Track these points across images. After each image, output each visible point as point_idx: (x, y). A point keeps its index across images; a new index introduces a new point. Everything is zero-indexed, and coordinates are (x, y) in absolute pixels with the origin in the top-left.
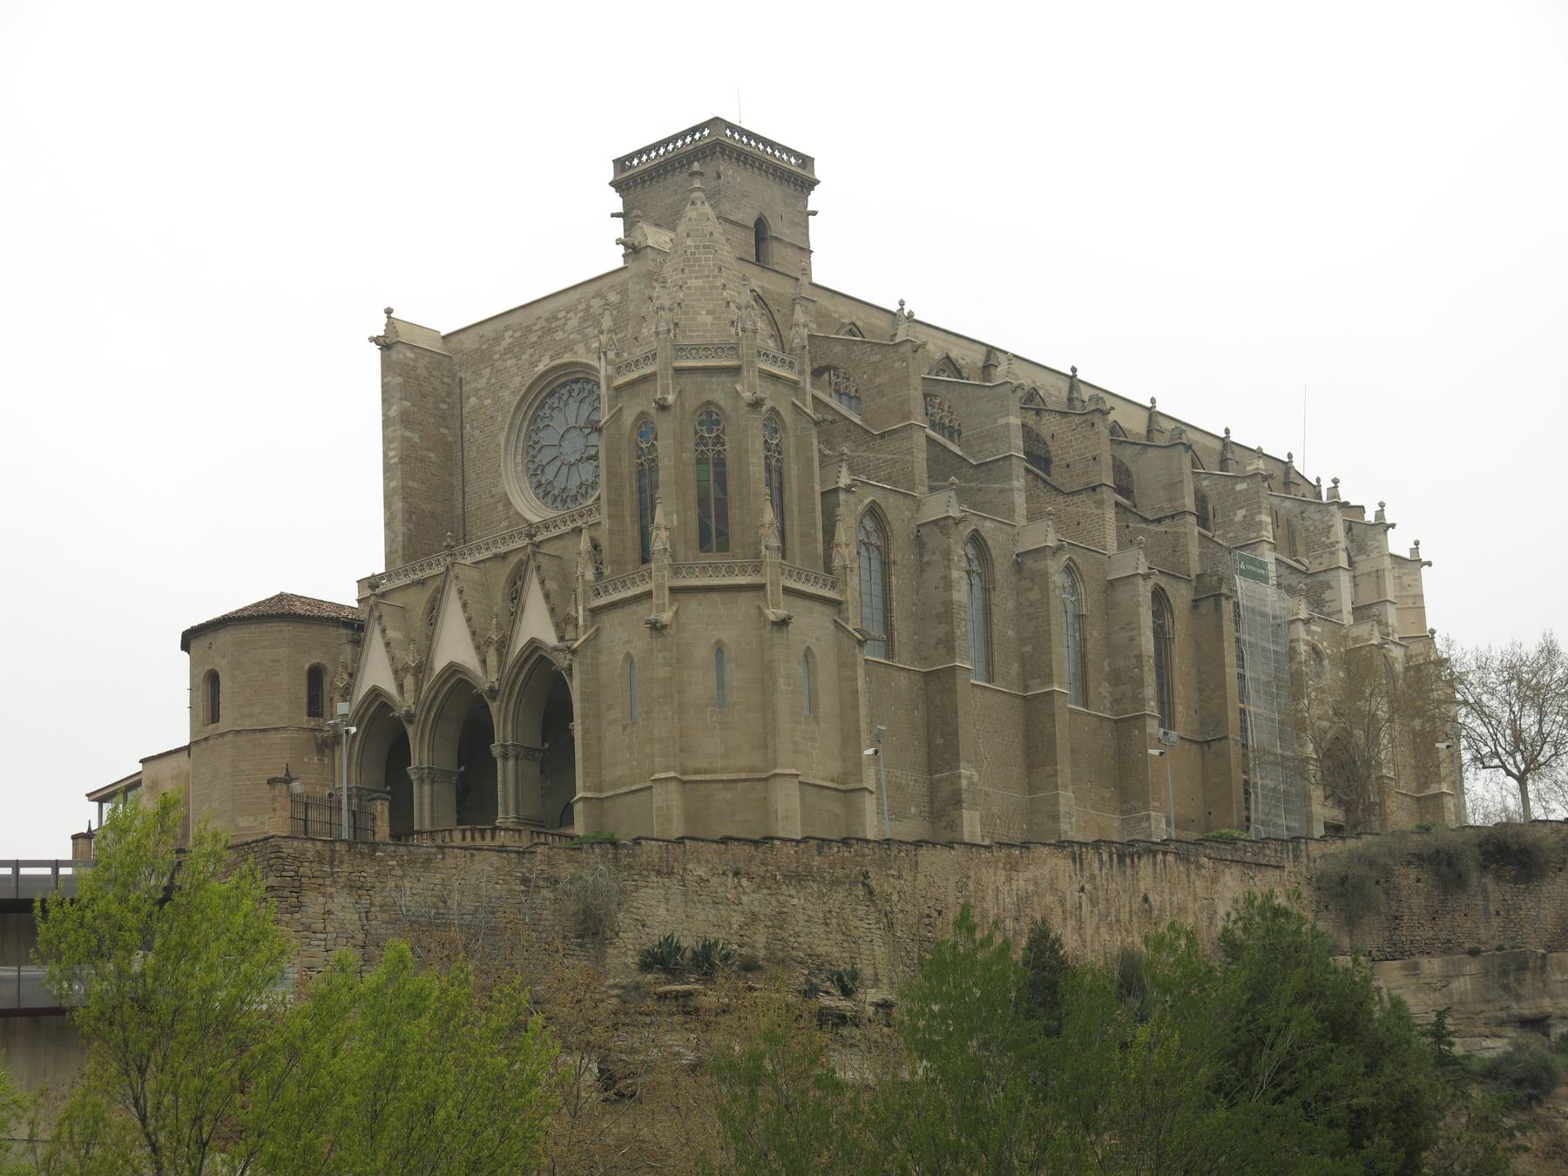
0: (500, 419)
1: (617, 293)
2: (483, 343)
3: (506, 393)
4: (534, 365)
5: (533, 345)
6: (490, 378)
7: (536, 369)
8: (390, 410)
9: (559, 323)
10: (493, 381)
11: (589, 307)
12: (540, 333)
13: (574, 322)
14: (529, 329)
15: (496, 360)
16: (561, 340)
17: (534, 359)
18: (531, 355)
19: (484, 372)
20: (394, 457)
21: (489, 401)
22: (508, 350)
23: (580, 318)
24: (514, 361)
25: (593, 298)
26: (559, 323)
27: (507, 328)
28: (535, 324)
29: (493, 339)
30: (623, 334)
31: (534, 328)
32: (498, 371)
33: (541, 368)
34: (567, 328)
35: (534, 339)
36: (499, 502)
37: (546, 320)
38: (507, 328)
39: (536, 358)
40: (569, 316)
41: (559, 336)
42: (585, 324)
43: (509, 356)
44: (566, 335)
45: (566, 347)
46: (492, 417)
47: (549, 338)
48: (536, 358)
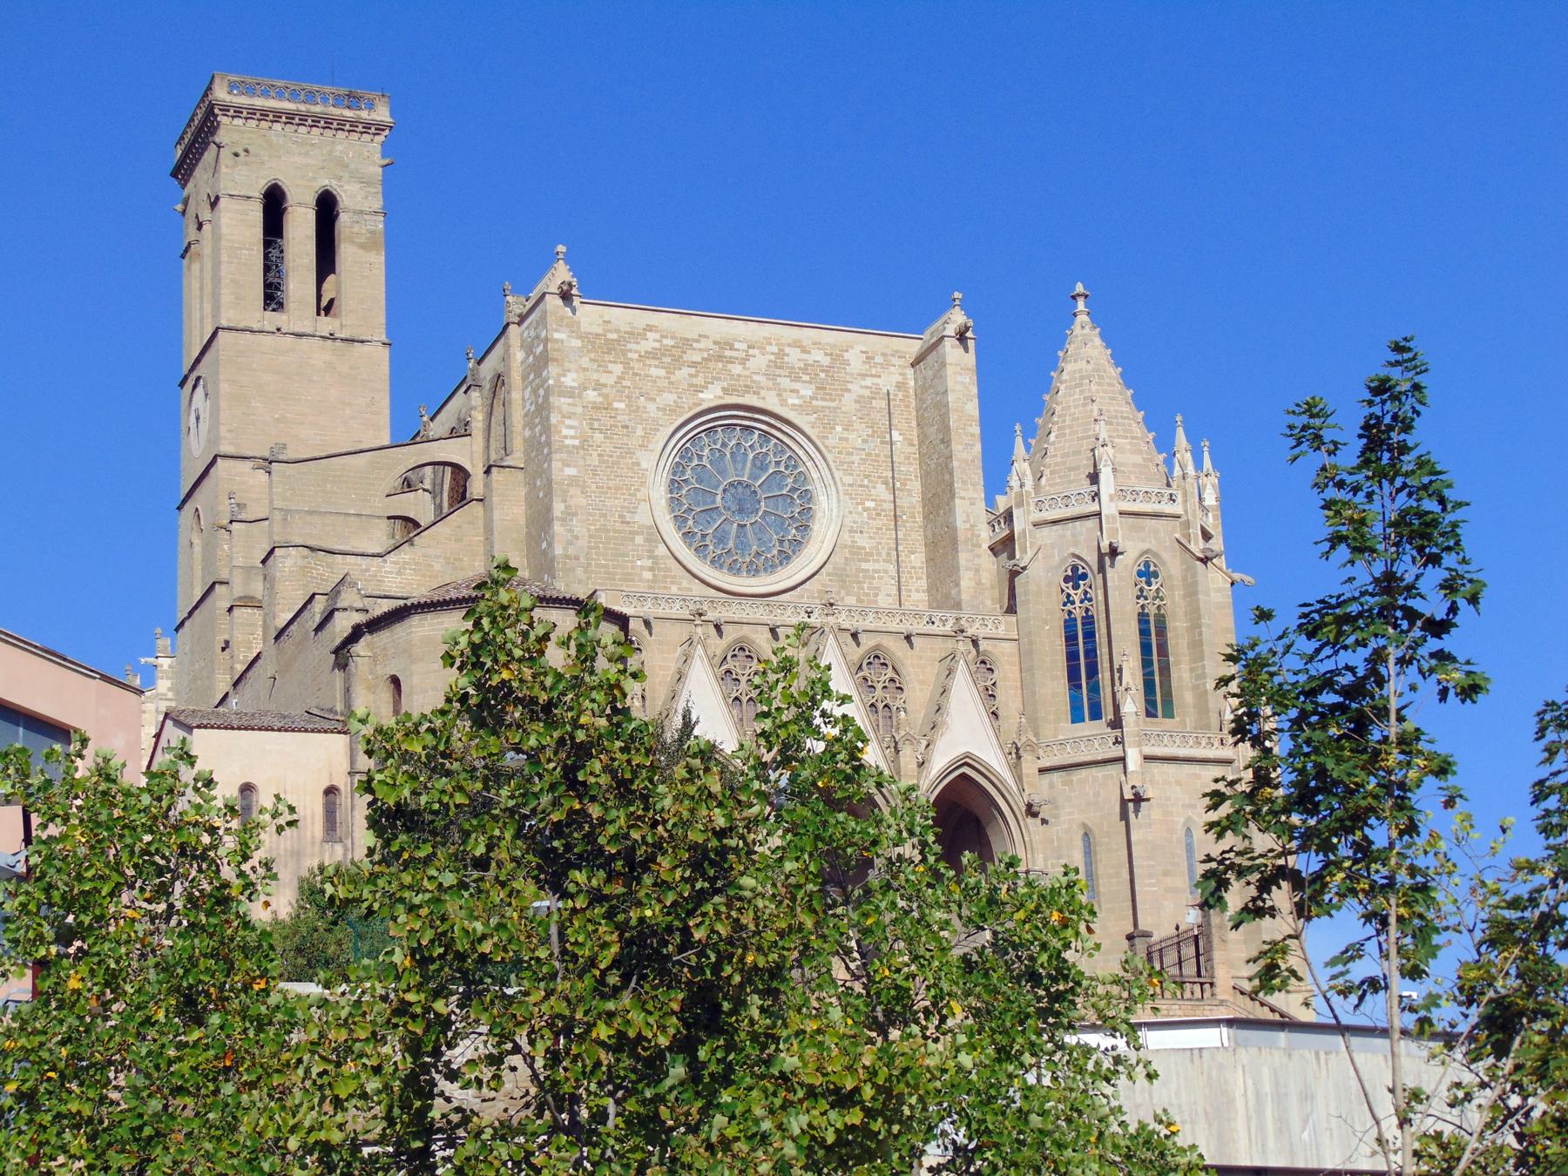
0: (640, 432)
1: (826, 354)
2: (611, 331)
3: (651, 407)
4: (698, 389)
5: (694, 364)
6: (621, 378)
7: (701, 395)
8: (565, 376)
9: (734, 354)
10: (625, 383)
11: (781, 354)
12: (705, 355)
13: (759, 361)
14: (686, 343)
15: (632, 360)
16: (739, 376)
17: (694, 381)
18: (691, 376)
19: (611, 367)
20: (572, 437)
21: (621, 406)
22: (652, 354)
23: (770, 361)
24: (662, 372)
25: (789, 345)
26: (734, 354)
27: (650, 328)
28: (698, 341)
29: (626, 333)
30: (834, 404)
31: (695, 345)
32: (635, 374)
33: (710, 397)
34: (748, 364)
35: (697, 358)
36: (637, 533)
37: (715, 343)
38: (650, 328)
39: (700, 380)
40: (751, 352)
41: (737, 369)
42: (778, 372)
43: (657, 363)
44: (748, 373)
45: (746, 386)
46: (627, 427)
47: (720, 365)
48: (700, 380)
